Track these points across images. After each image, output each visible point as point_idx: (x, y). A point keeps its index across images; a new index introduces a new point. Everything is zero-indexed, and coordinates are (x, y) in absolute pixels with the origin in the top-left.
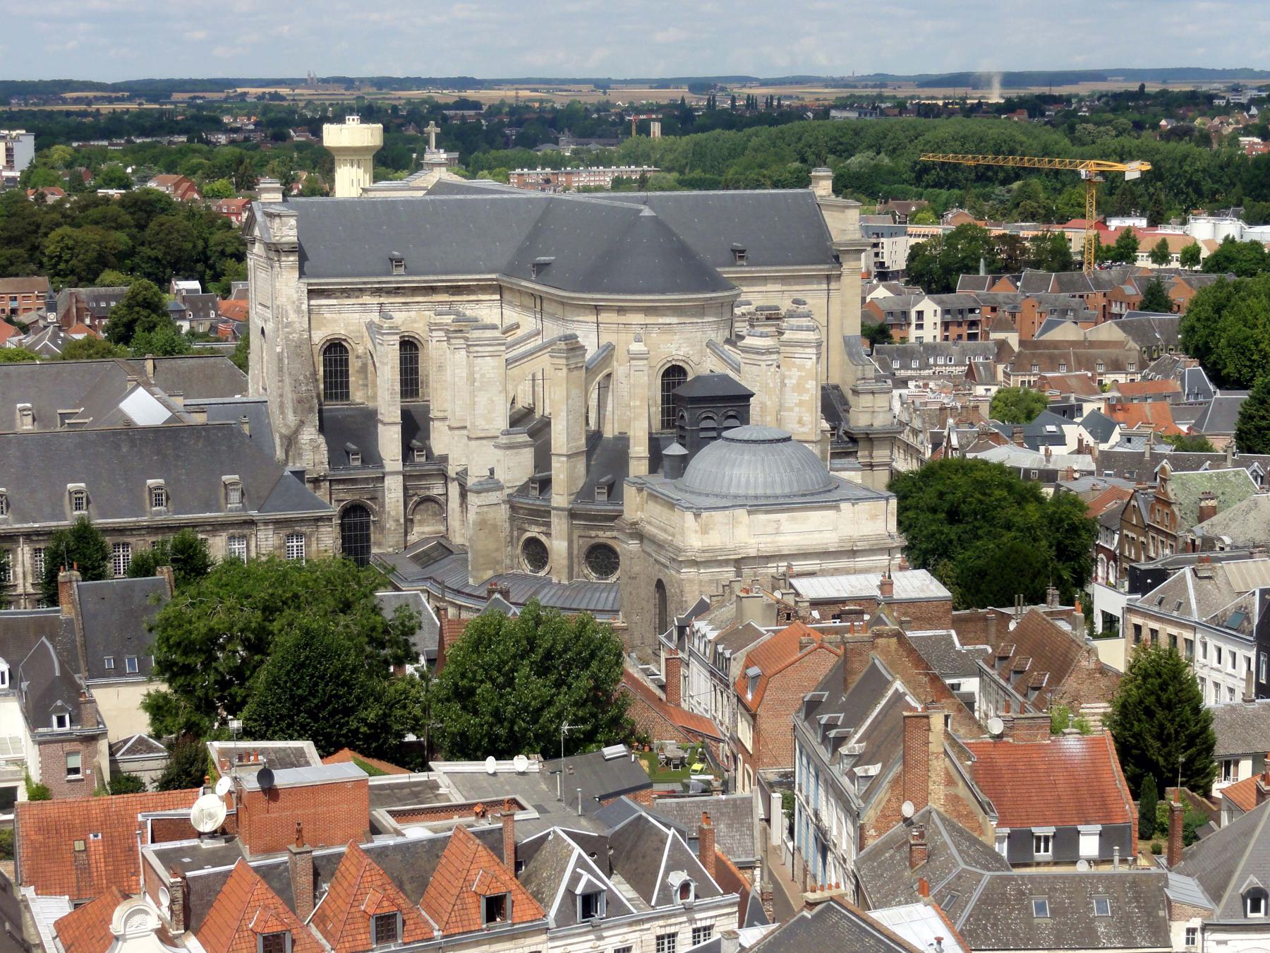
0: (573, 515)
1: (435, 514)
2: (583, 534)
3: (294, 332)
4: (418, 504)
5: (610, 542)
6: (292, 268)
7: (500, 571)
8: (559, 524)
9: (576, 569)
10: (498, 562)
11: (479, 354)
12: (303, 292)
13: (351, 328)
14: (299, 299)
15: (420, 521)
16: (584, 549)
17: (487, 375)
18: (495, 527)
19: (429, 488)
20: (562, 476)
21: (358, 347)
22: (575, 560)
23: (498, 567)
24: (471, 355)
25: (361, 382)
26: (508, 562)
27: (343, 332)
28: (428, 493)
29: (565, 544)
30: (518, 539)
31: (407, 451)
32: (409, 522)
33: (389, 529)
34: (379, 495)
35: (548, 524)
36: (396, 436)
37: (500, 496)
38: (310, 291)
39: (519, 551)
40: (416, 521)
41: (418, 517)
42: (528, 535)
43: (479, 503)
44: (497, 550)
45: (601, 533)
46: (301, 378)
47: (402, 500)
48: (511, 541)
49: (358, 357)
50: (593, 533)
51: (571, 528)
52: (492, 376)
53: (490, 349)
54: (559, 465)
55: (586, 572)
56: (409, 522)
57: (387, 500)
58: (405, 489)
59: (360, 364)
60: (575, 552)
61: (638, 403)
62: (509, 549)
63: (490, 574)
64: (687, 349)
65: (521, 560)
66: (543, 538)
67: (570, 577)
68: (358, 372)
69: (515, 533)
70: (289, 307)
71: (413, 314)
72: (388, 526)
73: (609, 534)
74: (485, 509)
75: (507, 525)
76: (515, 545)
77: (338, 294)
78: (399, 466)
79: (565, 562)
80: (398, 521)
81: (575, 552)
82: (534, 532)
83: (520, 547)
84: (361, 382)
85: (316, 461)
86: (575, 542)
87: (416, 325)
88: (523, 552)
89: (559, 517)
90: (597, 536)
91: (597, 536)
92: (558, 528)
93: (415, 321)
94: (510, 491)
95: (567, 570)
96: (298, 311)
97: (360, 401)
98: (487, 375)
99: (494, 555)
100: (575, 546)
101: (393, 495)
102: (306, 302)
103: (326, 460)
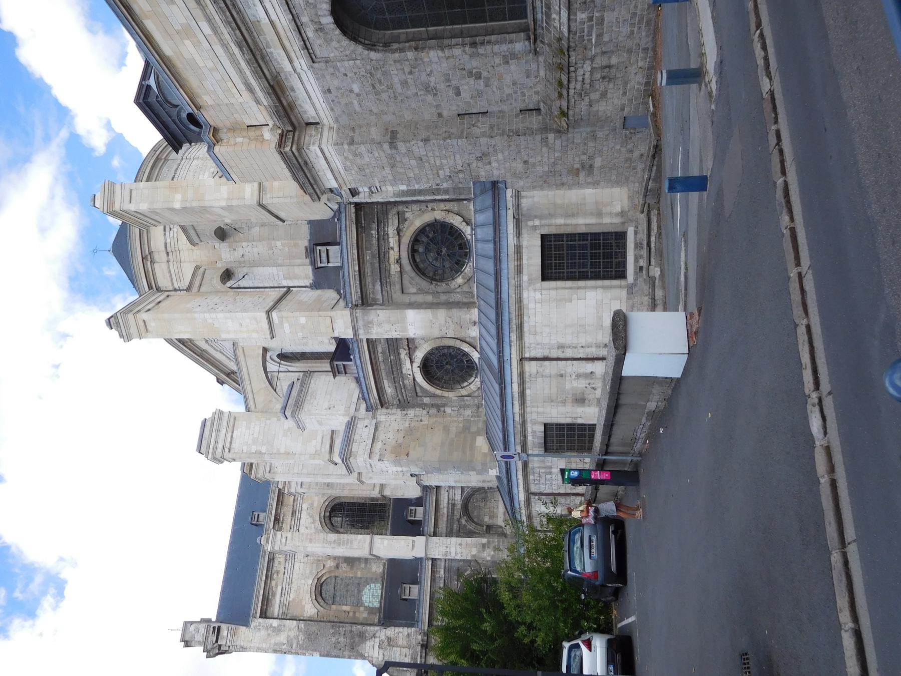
0: (365, 302)
1: (485, 499)
2: (398, 287)
3: (297, 637)
4: (470, 519)
5: (406, 239)
6: (235, 634)
7: (481, 425)
8: (380, 325)
9: (457, 297)
10: (466, 428)
11: (227, 445)
12: (260, 624)
13: (308, 572)
14: (267, 628)
15: (490, 518)
16: (424, 284)
17: (256, 435)
18: (410, 431)
19: (454, 505)
20: (303, 320)
21: (327, 566)
22: (443, 298)
23: (474, 429)
24: (227, 455)
25: (363, 565)
26: (468, 412)
27: (310, 582)
28: (459, 506)
29: (411, 315)
30: (434, 396)
31: (413, 528)
32: (490, 529)
33: (493, 557)
34: (455, 565)
35: (393, 344)
36: (386, 542)
37: (367, 422)
38: (264, 615)
39: (450, 394)
40: (491, 522)
41: (486, 519)
42: (420, 379)
43: (366, 456)
44: (446, 429)
45: (393, 255)
46: (333, 639)
47: (459, 540)
48: (438, 407)
49: (337, 567)
50: (394, 268)
51: (388, 302)
52: (257, 429)
53: (223, 432)
54: (286, 325)
55: (459, 280)
56: (490, 529)
57: (458, 557)
58: (449, 534)
59: (345, 565)
60: (429, 298)
61: (178, 197)
62: (448, 410)
63: (481, 442)
64: (207, 174)
65: (463, 392)
66: (419, 355)
67: (469, 305)
68: (352, 568)
69: (426, 400)
70: (273, 641)
71: (305, 506)
72: (489, 558)
73: (393, 241)
74: (378, 445)
75: (411, 412)
76: (444, 401)
77: (273, 583)
78: (420, 540)
79: (442, 314)
80: (484, 546)
81: (429, 298)
82: (412, 370)
83: (445, 394)
84: (363, 565)
85: (405, 643)
86: (414, 298)
87: (316, 504)
88: (452, 389)
89: (368, 325)
90: (398, 261)
91: (398, 261)
92: (387, 327)
93: (312, 505)
94: (363, 406)
95: (455, 312)
96: (278, 630)
97: (382, 567)
98: (256, 435)
99: (452, 435)
100: (420, 298)
101: (453, 550)
102: (271, 621)
103: (406, 631)
